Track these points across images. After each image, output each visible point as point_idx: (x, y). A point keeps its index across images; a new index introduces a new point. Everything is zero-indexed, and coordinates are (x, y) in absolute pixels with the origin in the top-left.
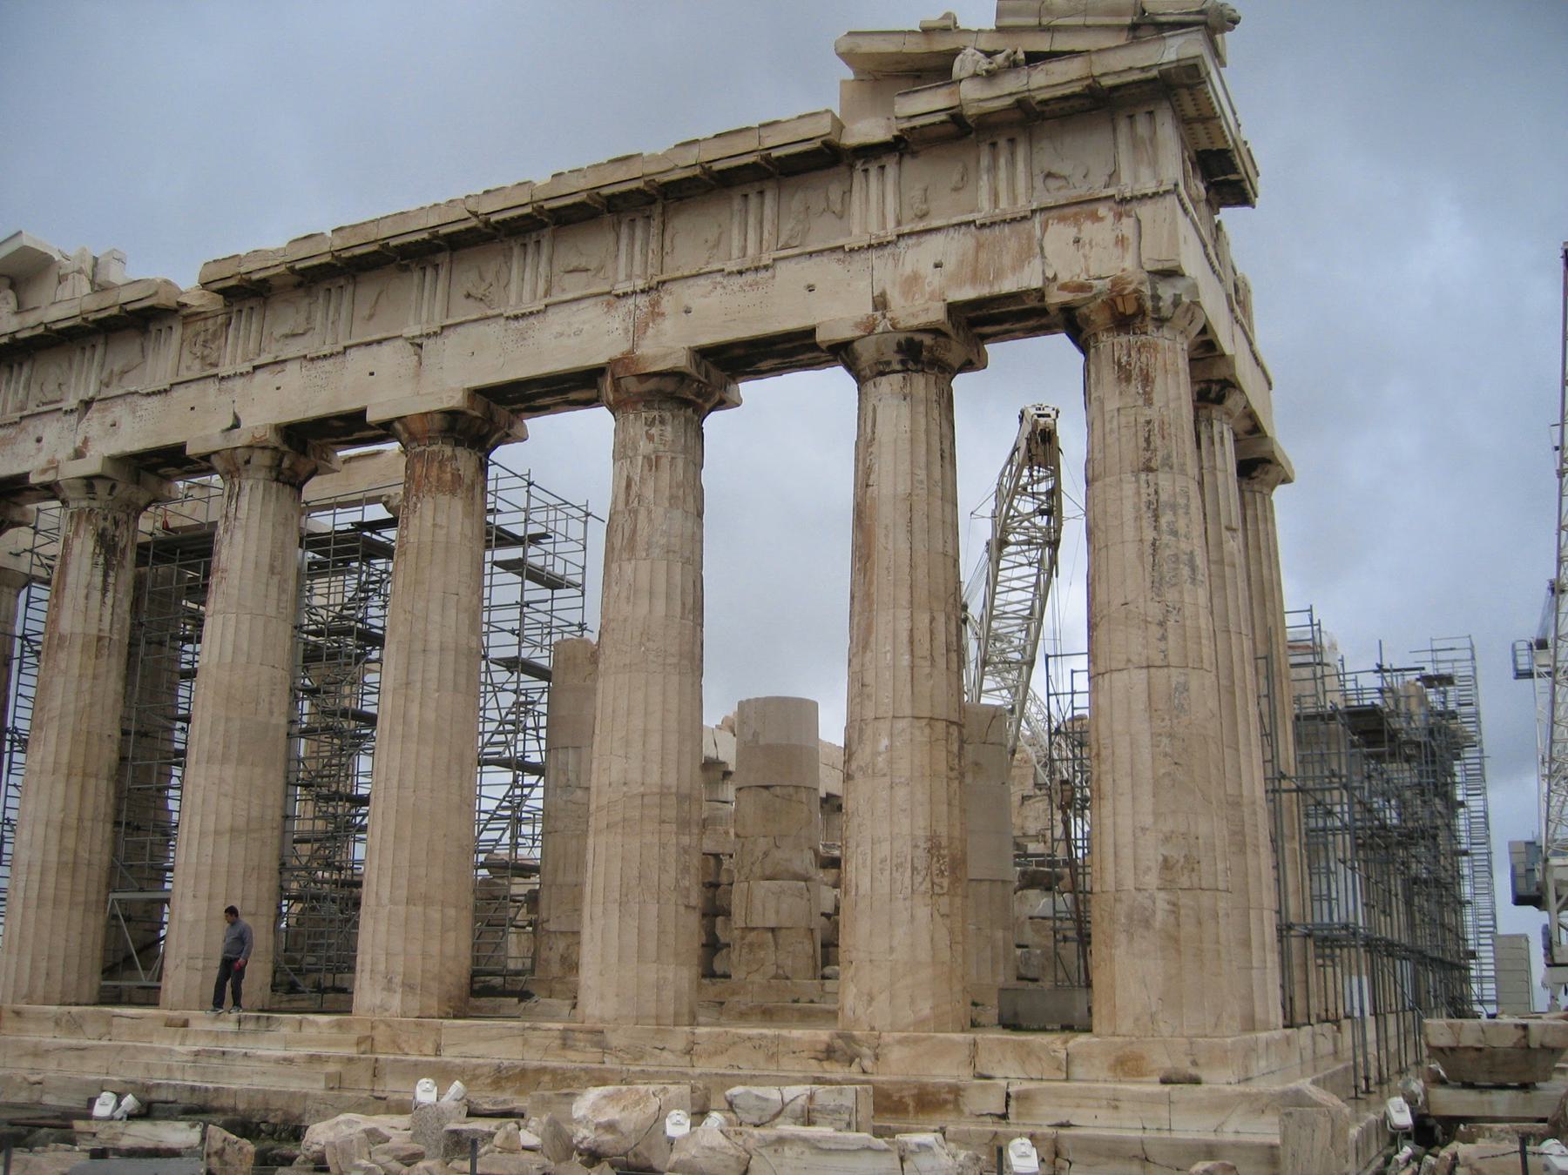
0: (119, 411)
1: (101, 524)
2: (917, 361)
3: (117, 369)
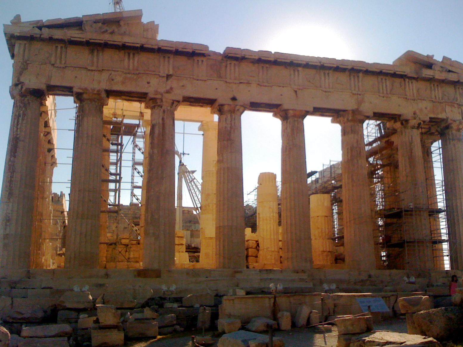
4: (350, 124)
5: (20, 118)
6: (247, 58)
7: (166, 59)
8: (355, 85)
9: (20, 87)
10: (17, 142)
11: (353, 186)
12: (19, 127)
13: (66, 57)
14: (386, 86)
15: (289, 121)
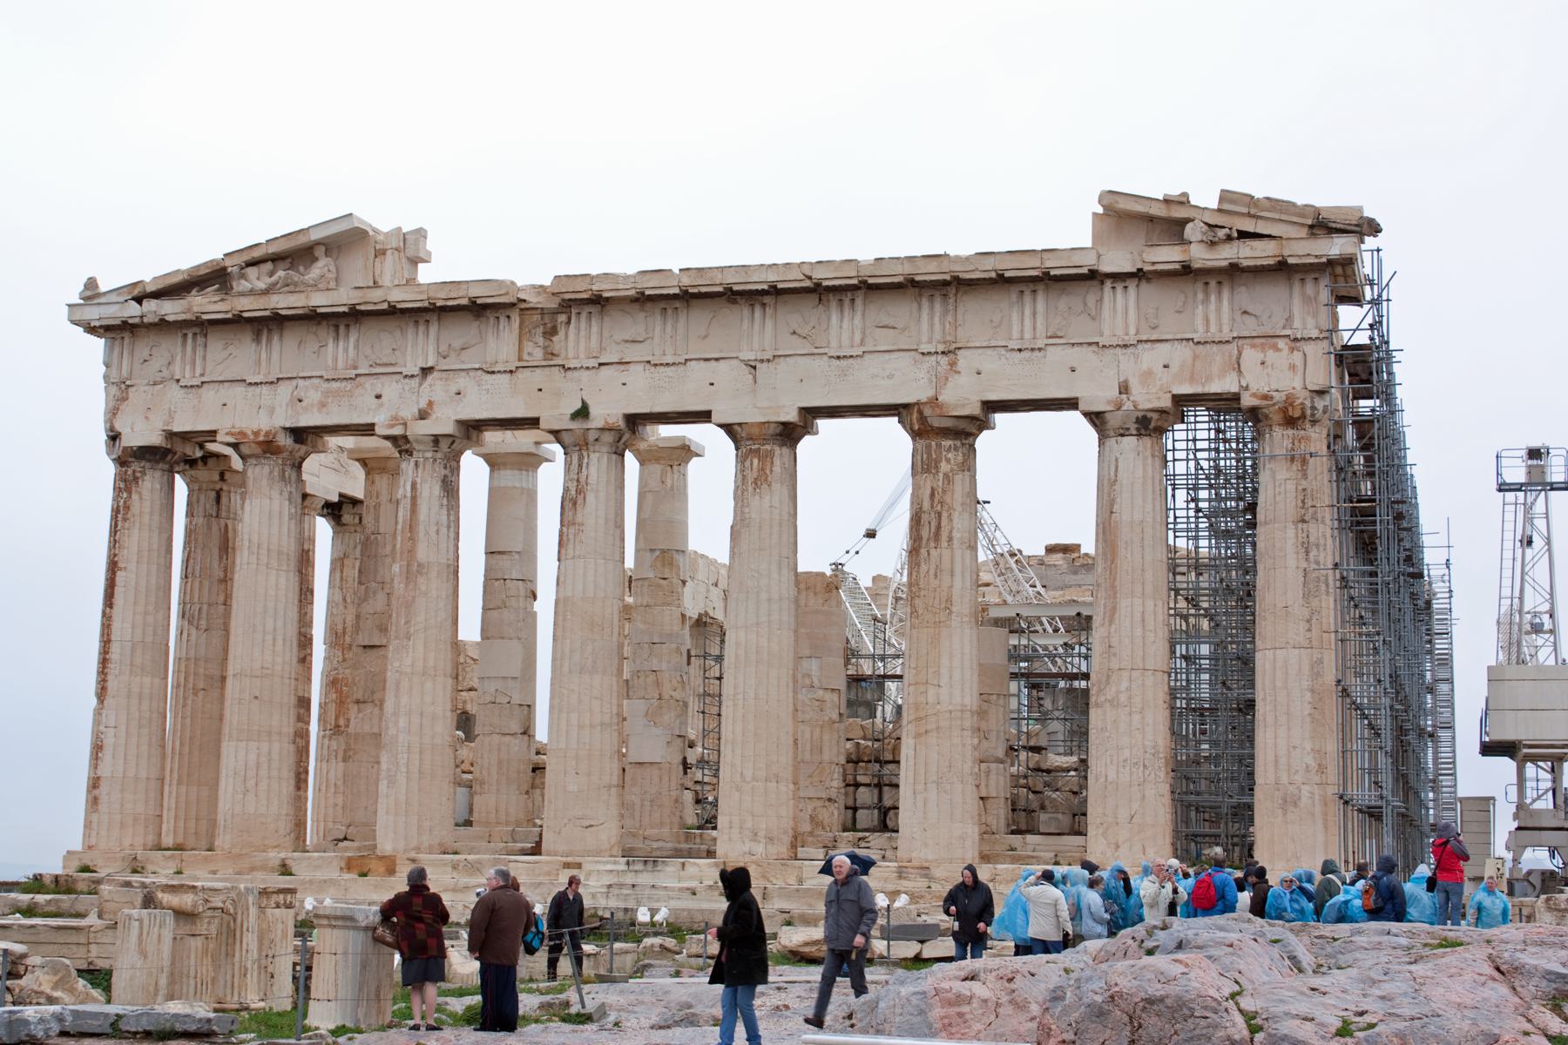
0: (462, 382)
1: (444, 472)
2: (1146, 428)
3: (457, 344)
4: (922, 443)
7: (422, 328)
8: (932, 325)
13: (204, 358)
14: (1034, 314)
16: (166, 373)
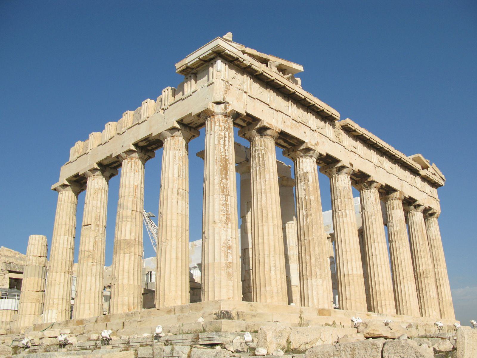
4: (397, 201)
5: (227, 139)
6: (357, 132)
9: (222, 106)
10: (226, 164)
11: (403, 251)
12: (226, 147)
15: (372, 190)
16: (241, 87)
